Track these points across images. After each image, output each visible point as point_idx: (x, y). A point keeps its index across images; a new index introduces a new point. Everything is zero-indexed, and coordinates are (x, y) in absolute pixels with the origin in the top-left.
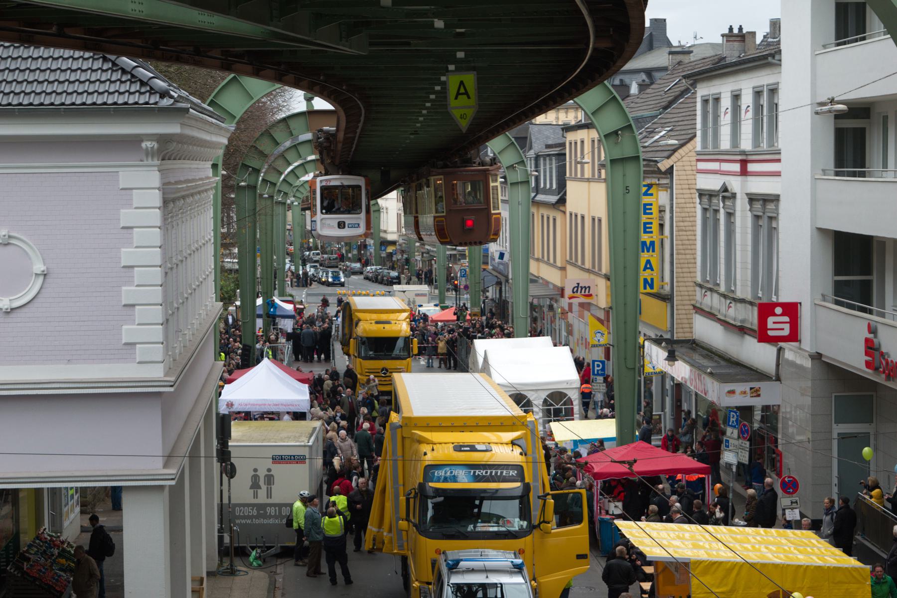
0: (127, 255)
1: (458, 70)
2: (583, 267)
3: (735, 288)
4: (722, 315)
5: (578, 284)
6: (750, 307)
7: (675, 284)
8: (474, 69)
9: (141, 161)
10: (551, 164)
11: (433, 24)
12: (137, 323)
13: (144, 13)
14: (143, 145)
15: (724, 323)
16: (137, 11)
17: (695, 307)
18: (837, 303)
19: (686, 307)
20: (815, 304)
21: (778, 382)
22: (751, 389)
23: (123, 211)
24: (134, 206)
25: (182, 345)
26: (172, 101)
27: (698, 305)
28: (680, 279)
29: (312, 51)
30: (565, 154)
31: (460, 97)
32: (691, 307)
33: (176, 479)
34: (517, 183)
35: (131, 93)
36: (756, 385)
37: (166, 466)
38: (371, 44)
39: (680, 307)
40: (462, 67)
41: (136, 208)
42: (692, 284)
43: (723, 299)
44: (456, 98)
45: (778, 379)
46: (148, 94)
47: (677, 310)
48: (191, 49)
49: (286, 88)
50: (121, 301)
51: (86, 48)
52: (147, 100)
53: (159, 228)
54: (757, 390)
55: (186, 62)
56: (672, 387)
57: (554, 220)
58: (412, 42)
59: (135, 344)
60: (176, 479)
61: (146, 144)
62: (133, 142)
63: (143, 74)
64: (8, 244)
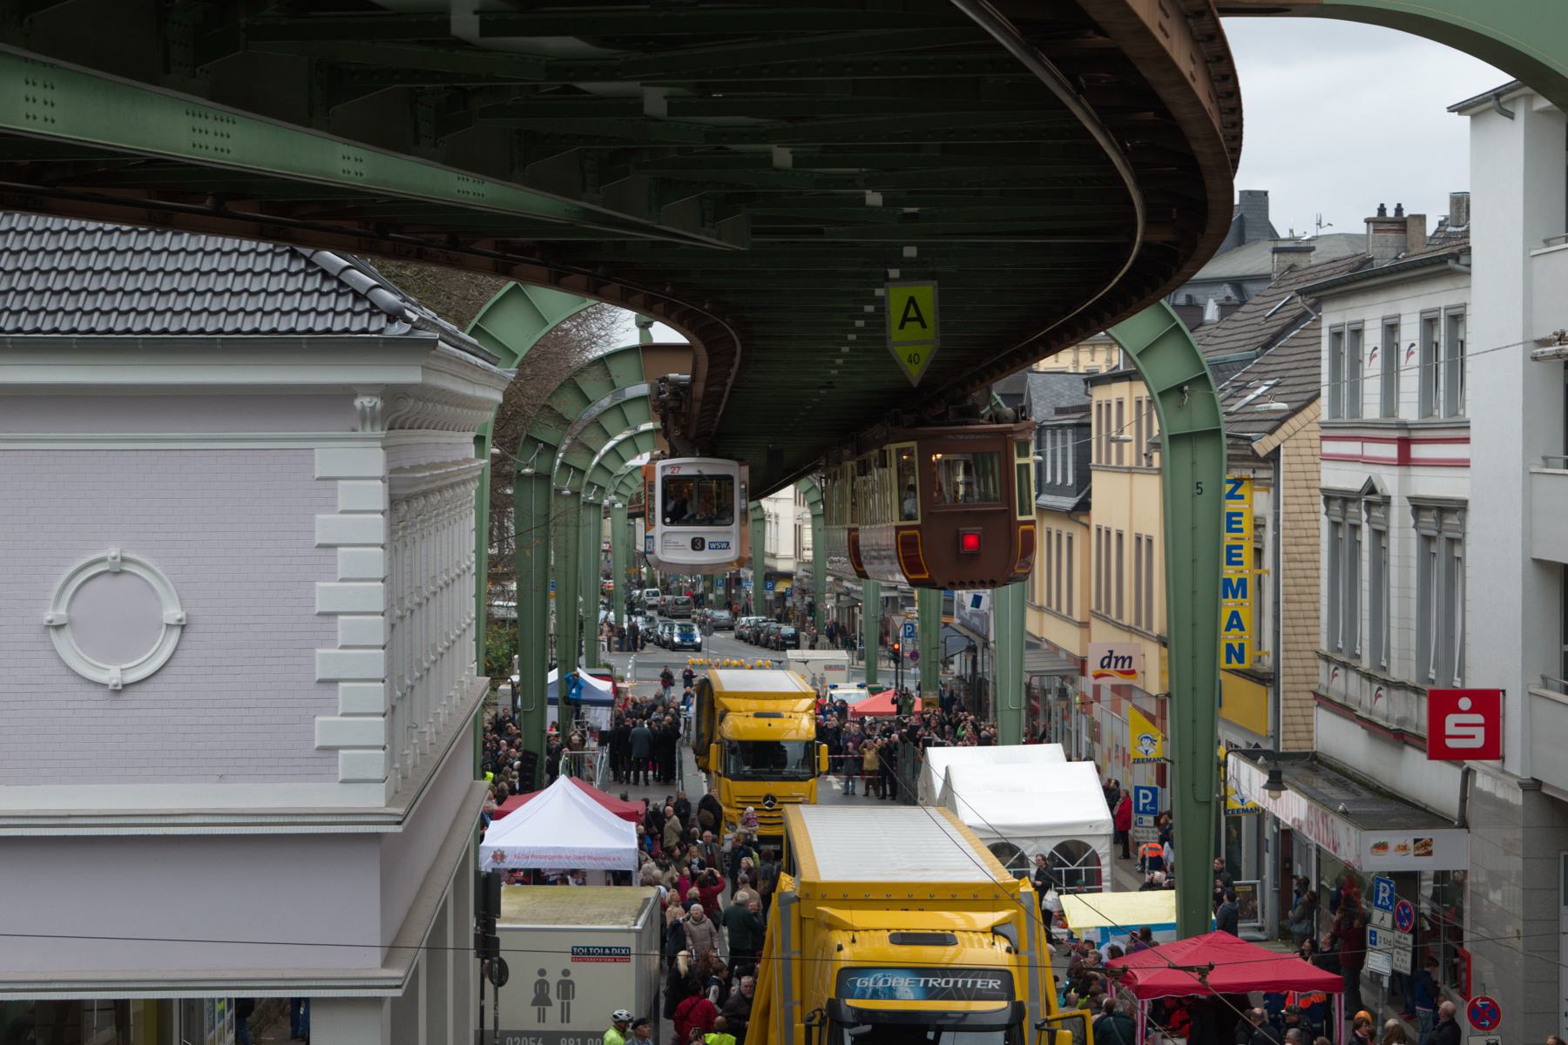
0: (326, 594)
1: (906, 278)
2: (1120, 621)
3: (1389, 662)
4: (1365, 709)
5: (1111, 652)
6: (1414, 697)
8: (932, 276)
9: (354, 431)
10: (1064, 442)
11: (865, 199)
12: (340, 713)
13: (364, 176)
14: (358, 403)
15: (1369, 725)
16: (353, 172)
17: (1316, 695)
19: (1301, 695)
20: (1530, 693)
21: (1465, 830)
22: (1416, 841)
23: (319, 517)
24: (340, 508)
25: (418, 751)
26: (408, 327)
27: (1322, 692)
28: (1290, 646)
29: (652, 242)
30: (1089, 425)
31: (908, 324)
32: (1312, 696)
33: (404, 987)
35: (337, 314)
36: (1425, 834)
37: (386, 963)
38: (755, 233)
39: (1290, 695)
40: (913, 273)
41: (343, 512)
42: (1311, 655)
43: (1366, 683)
44: (902, 326)
45: (1464, 824)
46: (366, 315)
47: (1285, 699)
48: (444, 238)
49: (606, 305)
50: (314, 673)
51: (260, 236)
52: (365, 325)
53: (383, 547)
54: (1428, 844)
55: (435, 261)
56: (1276, 835)
57: (1070, 539)
58: (825, 229)
59: (336, 749)
60: (404, 987)
61: (363, 402)
62: (340, 397)
63: (359, 281)
64: (122, 572)
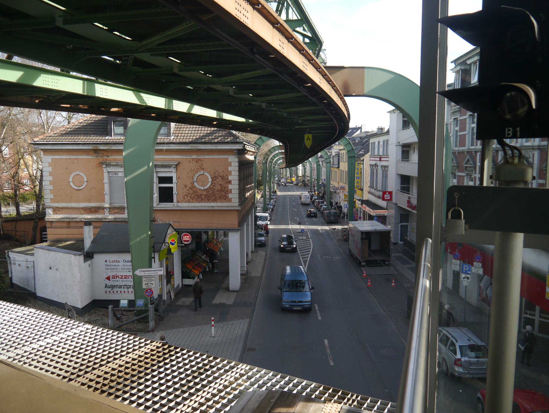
1: (308, 134)
18: (401, 192)
40: (309, 133)
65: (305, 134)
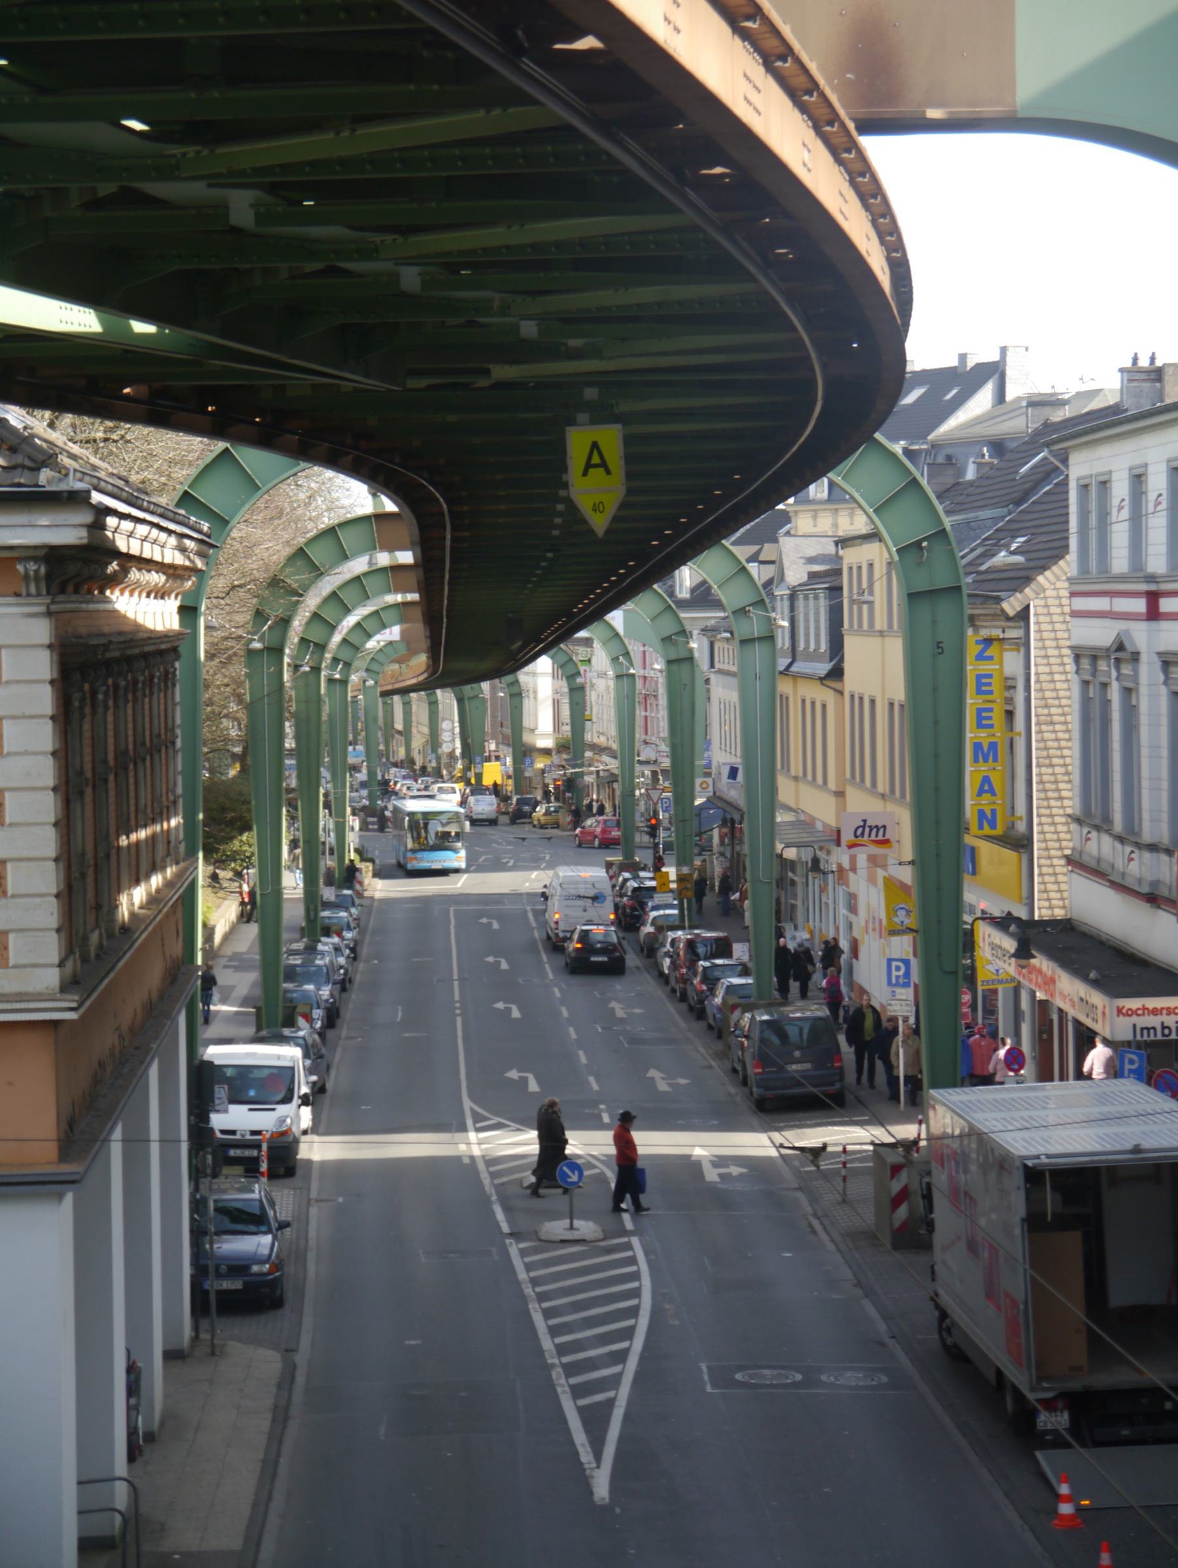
1: (594, 421)
5: (865, 821)
7: (1035, 820)
30: (841, 589)
31: (591, 471)
32: (1063, 862)
34: (752, 640)
43: (1118, 845)
44: (585, 474)
49: (303, 465)
65: (572, 422)
